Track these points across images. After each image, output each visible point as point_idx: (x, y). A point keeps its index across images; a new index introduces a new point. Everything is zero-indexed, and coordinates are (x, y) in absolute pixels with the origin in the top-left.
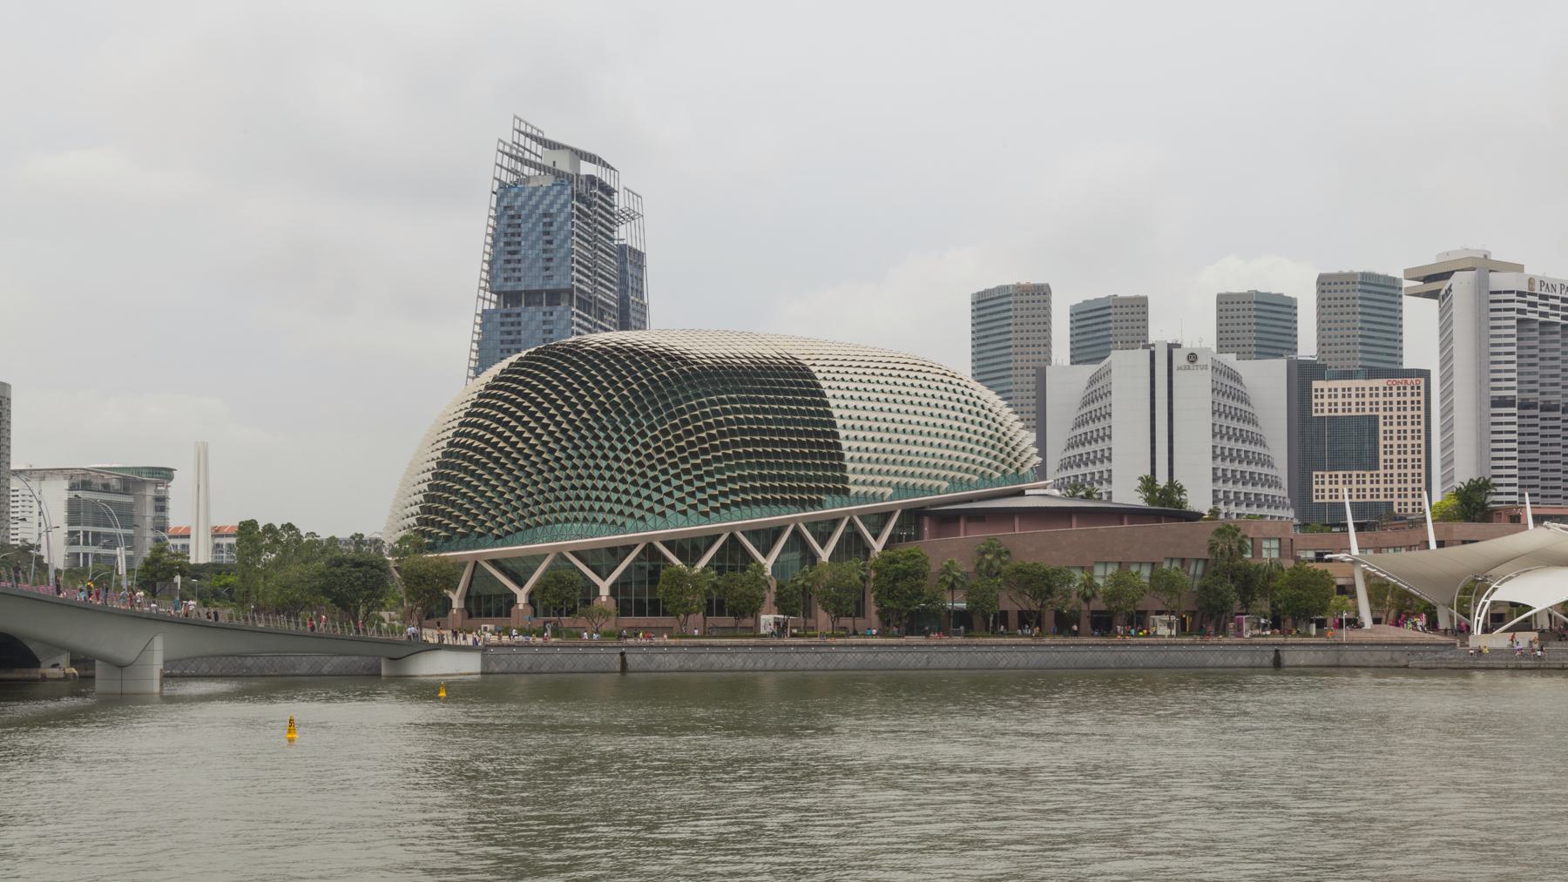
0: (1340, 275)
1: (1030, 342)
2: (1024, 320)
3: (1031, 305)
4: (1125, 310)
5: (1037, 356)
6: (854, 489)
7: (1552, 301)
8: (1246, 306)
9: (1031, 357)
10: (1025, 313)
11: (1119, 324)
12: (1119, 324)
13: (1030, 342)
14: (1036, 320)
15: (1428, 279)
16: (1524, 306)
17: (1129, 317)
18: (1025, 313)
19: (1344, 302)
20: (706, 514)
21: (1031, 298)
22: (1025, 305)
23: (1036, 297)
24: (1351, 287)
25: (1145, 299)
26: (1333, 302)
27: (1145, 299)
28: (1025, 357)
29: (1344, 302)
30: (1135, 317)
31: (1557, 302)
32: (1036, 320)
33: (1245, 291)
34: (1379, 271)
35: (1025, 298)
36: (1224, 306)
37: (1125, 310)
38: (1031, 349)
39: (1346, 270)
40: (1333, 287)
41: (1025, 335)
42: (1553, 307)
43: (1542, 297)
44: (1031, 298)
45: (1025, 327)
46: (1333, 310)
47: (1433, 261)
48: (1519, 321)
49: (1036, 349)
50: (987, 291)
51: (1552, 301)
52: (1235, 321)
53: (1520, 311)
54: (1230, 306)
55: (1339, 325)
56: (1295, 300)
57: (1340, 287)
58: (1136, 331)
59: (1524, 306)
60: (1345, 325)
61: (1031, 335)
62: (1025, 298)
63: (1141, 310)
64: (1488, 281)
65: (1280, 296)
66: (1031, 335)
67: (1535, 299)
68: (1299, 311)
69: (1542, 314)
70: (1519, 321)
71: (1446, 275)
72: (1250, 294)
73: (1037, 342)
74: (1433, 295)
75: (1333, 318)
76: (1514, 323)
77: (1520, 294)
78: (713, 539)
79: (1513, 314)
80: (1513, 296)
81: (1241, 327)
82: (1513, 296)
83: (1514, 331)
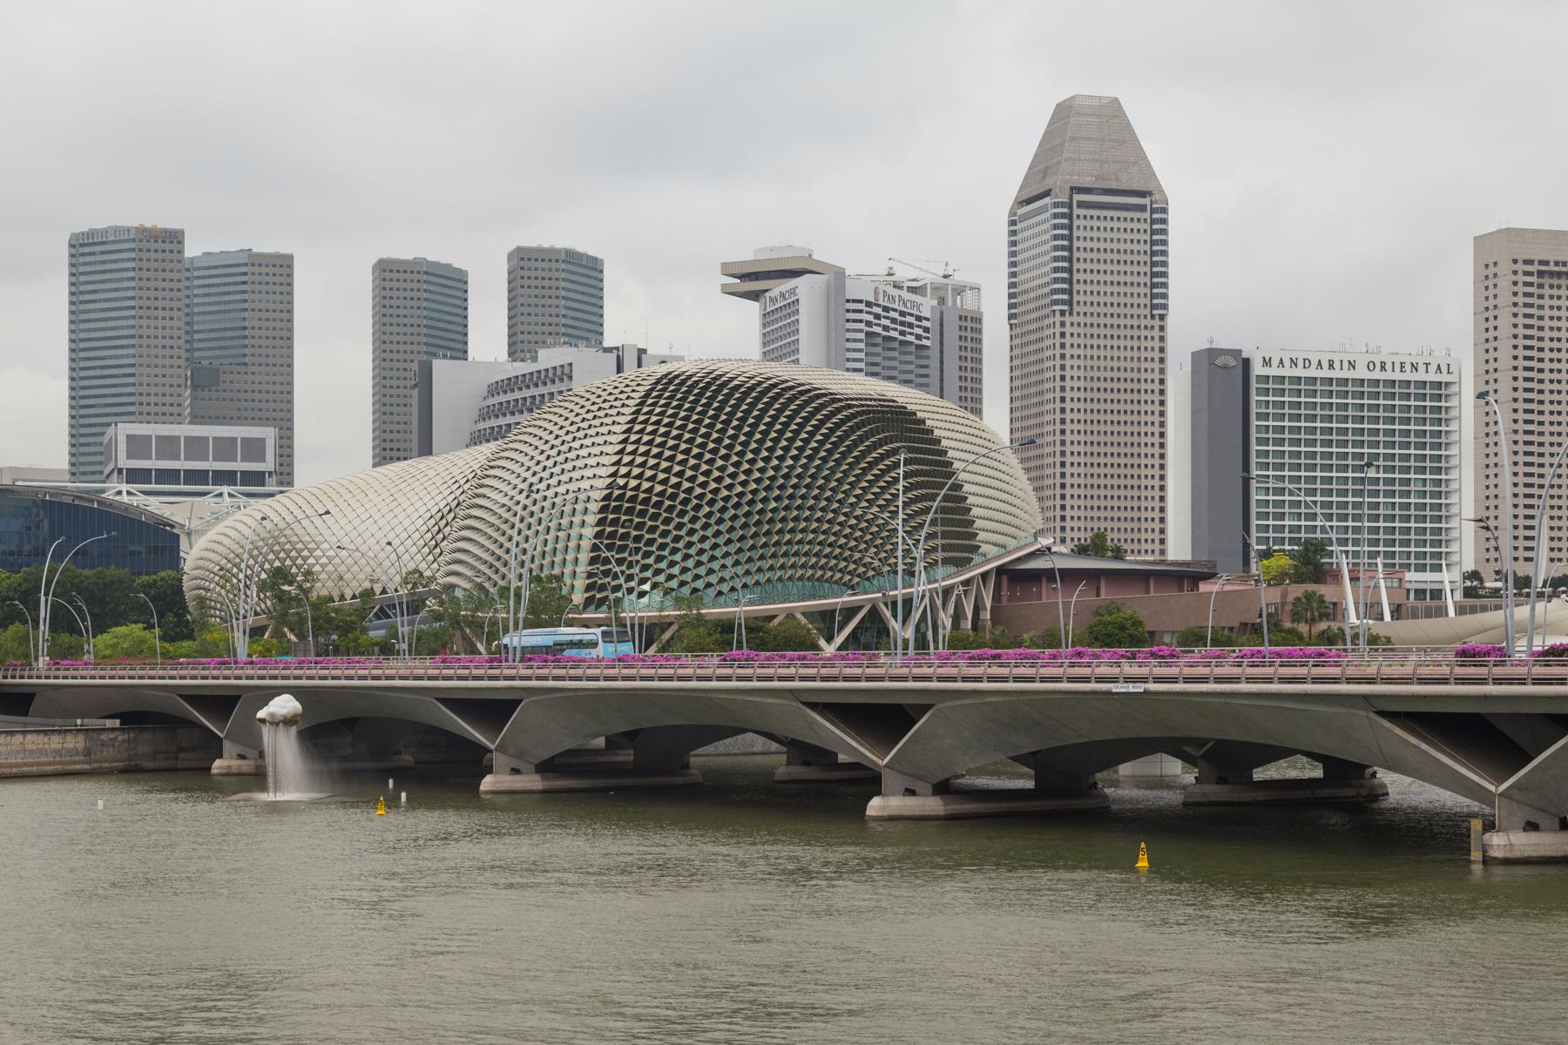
1: (160, 304)
2: (152, 274)
3: (160, 256)
4: (265, 270)
5: (168, 323)
6: (984, 548)
8: (415, 277)
9: (160, 323)
10: (153, 265)
11: (257, 288)
12: (257, 288)
13: (160, 304)
14: (168, 275)
15: (745, 277)
16: (870, 318)
17: (270, 279)
18: (153, 265)
19: (547, 283)
21: (160, 246)
22: (153, 255)
23: (168, 246)
24: (553, 265)
25: (290, 258)
26: (533, 283)
27: (290, 258)
28: (153, 323)
29: (547, 283)
30: (277, 279)
32: (168, 275)
33: (411, 258)
34: (580, 249)
35: (152, 246)
36: (387, 275)
37: (265, 270)
38: (160, 313)
39: (546, 245)
40: (533, 264)
41: (152, 294)
42: (894, 321)
43: (886, 309)
44: (160, 246)
45: (152, 284)
46: (533, 291)
48: (868, 334)
49: (167, 314)
50: (92, 233)
52: (401, 294)
53: (869, 324)
54: (395, 276)
55: (540, 310)
56: (465, 273)
57: (540, 265)
58: (278, 297)
59: (870, 318)
60: (547, 310)
61: (159, 294)
62: (152, 246)
63: (285, 271)
64: (844, 288)
65: (448, 266)
66: (159, 294)
67: (878, 310)
68: (471, 287)
69: (886, 328)
70: (868, 334)
72: (417, 262)
73: (168, 304)
74: (755, 296)
75: (533, 301)
76: (862, 336)
77: (869, 304)
79: (862, 326)
80: (862, 306)
81: (409, 303)
82: (862, 306)
83: (862, 346)
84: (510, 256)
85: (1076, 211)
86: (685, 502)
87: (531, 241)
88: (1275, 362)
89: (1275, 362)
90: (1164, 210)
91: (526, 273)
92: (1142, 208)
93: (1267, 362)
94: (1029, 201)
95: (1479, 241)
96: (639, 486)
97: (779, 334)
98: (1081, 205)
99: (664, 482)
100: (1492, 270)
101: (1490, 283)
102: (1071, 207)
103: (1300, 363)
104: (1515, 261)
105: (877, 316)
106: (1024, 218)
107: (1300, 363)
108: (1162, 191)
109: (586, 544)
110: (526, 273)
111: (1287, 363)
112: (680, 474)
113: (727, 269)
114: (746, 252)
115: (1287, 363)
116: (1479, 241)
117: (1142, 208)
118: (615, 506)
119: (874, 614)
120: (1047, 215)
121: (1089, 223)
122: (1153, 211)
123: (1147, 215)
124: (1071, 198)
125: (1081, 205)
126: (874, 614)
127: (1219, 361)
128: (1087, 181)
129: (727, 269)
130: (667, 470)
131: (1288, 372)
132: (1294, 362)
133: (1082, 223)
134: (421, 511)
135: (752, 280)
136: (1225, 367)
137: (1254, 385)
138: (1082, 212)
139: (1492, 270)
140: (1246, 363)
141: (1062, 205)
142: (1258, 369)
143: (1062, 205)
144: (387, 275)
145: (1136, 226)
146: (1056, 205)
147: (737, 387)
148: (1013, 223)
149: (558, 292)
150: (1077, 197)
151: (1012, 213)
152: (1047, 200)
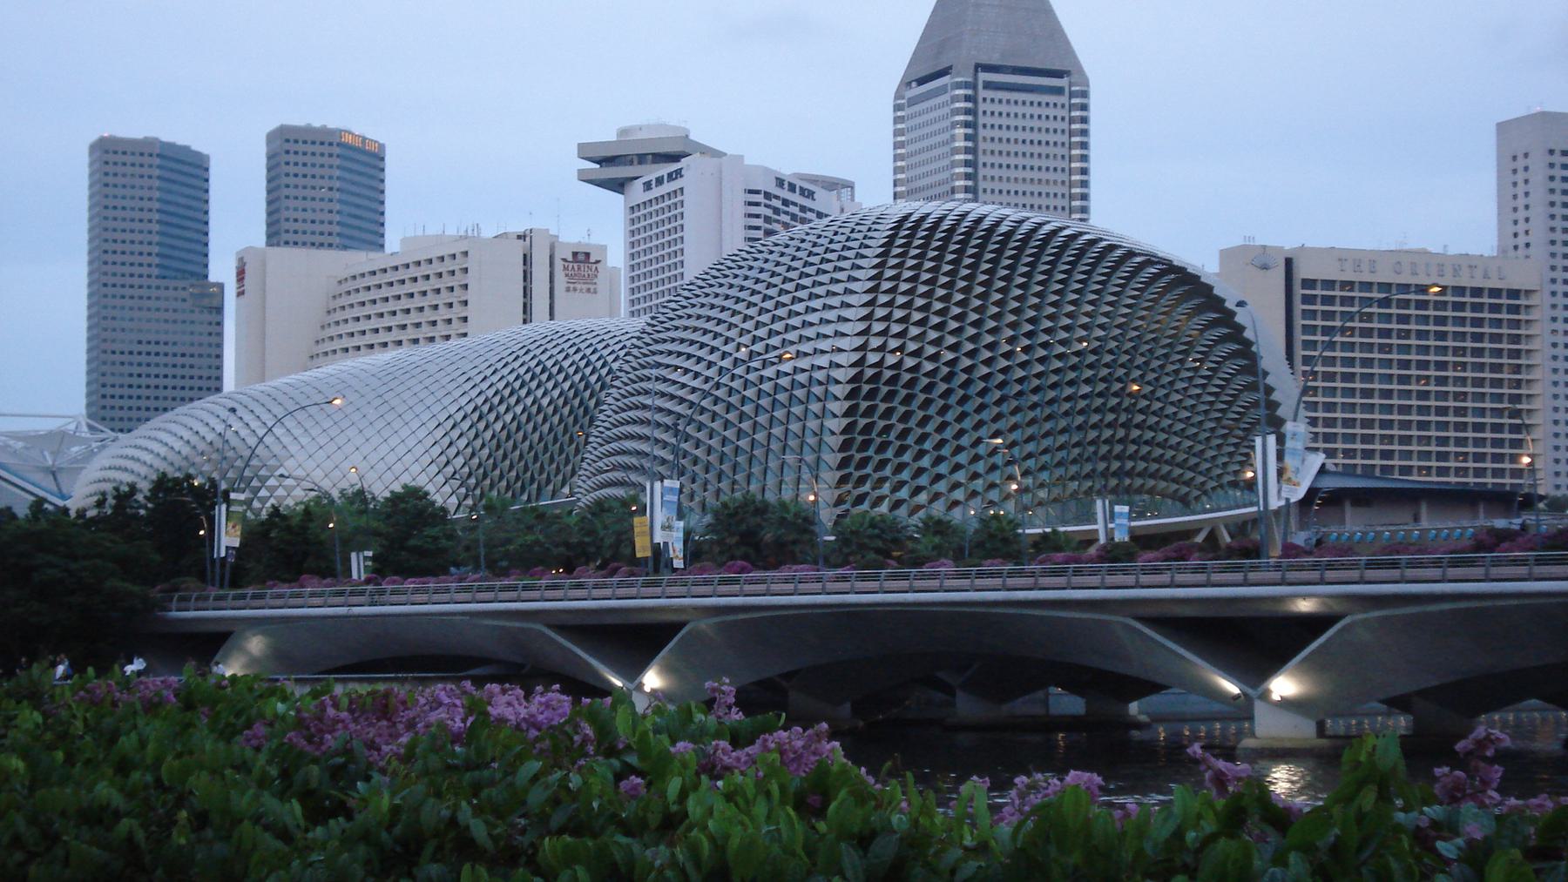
0: (308, 129)
7: (792, 209)
16: (769, 212)
31: (795, 210)
33: (138, 134)
36: (111, 158)
39: (317, 124)
40: (301, 147)
47: (613, 138)
51: (792, 209)
53: (767, 220)
54: (120, 158)
56: (207, 157)
59: (769, 212)
65: (186, 149)
67: (777, 203)
71: (674, 158)
74: (618, 186)
77: (768, 195)
80: (760, 198)
82: (760, 198)
84: (271, 137)
85: (982, 93)
86: (966, 384)
87: (297, 119)
90: (1085, 94)
91: (292, 158)
92: (1059, 91)
94: (922, 81)
95: (1502, 128)
96: (901, 362)
97: (655, 231)
98: (988, 85)
99: (934, 358)
100: (1521, 163)
101: (1520, 177)
102: (974, 87)
104: (1551, 152)
105: (776, 211)
106: (913, 102)
108: (1081, 71)
109: (835, 441)
110: (292, 158)
112: (954, 348)
113: (585, 152)
114: (605, 133)
116: (1502, 128)
117: (1059, 91)
118: (867, 387)
120: (946, 97)
121: (997, 108)
122: (1072, 95)
123: (1063, 99)
124: (976, 78)
125: (988, 85)
128: (995, 59)
129: (585, 152)
130: (937, 342)
133: (988, 107)
134: (425, 417)
135: (612, 166)
137: (1299, 292)
138: (990, 94)
139: (1521, 163)
141: (966, 85)
142: (1303, 272)
143: (966, 85)
144: (111, 158)
145: (1051, 112)
146: (958, 86)
147: (1008, 235)
148: (897, 108)
149: (329, 183)
150: (984, 76)
151: (898, 95)
152: (945, 80)
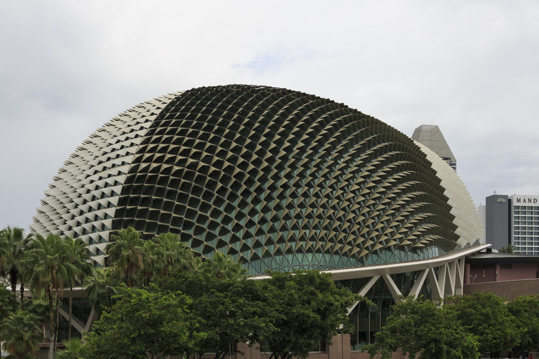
20: (414, 250)
78: (367, 280)
88: (522, 200)
89: (522, 200)
93: (518, 200)
103: (532, 201)
107: (532, 201)
111: (527, 200)
115: (527, 200)
119: (382, 282)
126: (382, 282)
127: (499, 200)
131: (527, 204)
132: (530, 200)
136: (501, 203)
137: (513, 210)
140: (510, 201)
142: (515, 203)
